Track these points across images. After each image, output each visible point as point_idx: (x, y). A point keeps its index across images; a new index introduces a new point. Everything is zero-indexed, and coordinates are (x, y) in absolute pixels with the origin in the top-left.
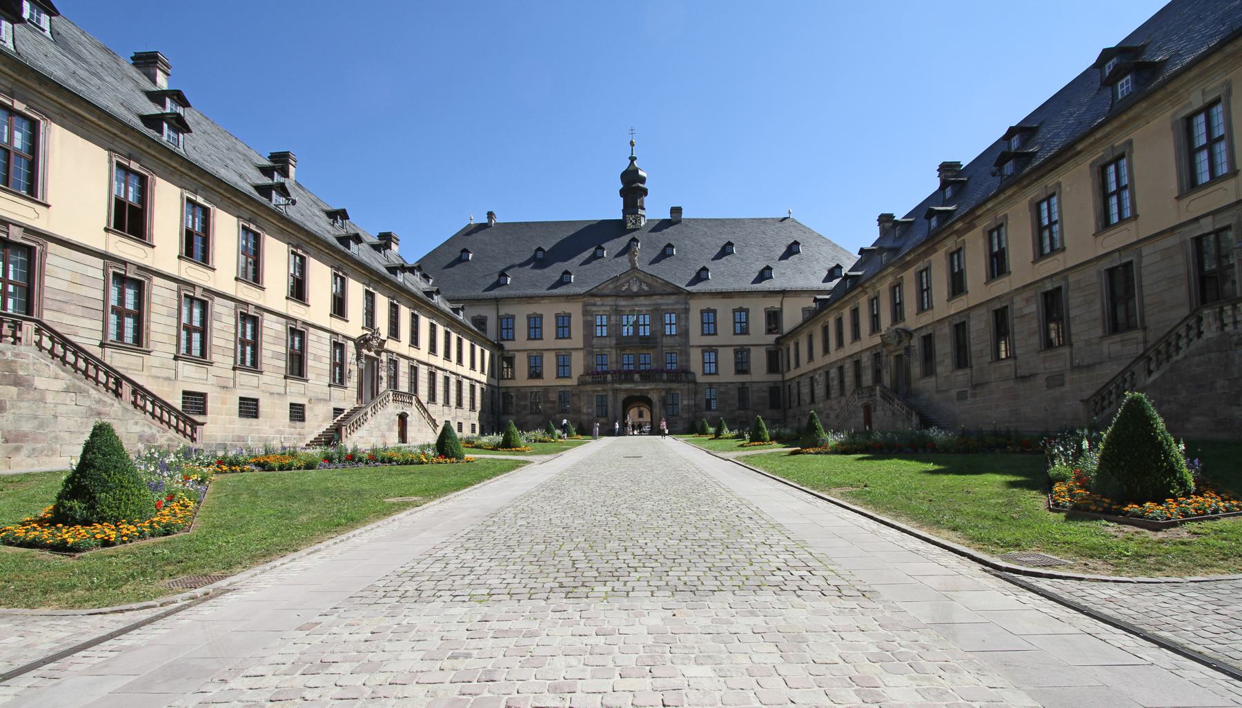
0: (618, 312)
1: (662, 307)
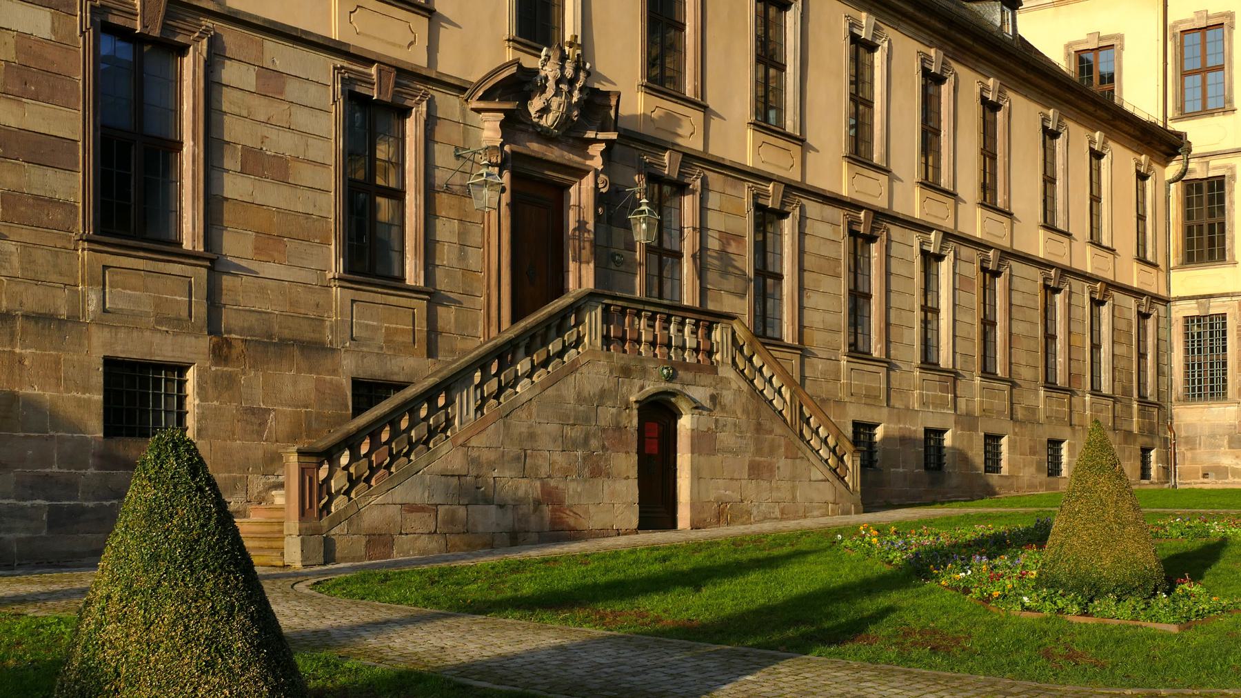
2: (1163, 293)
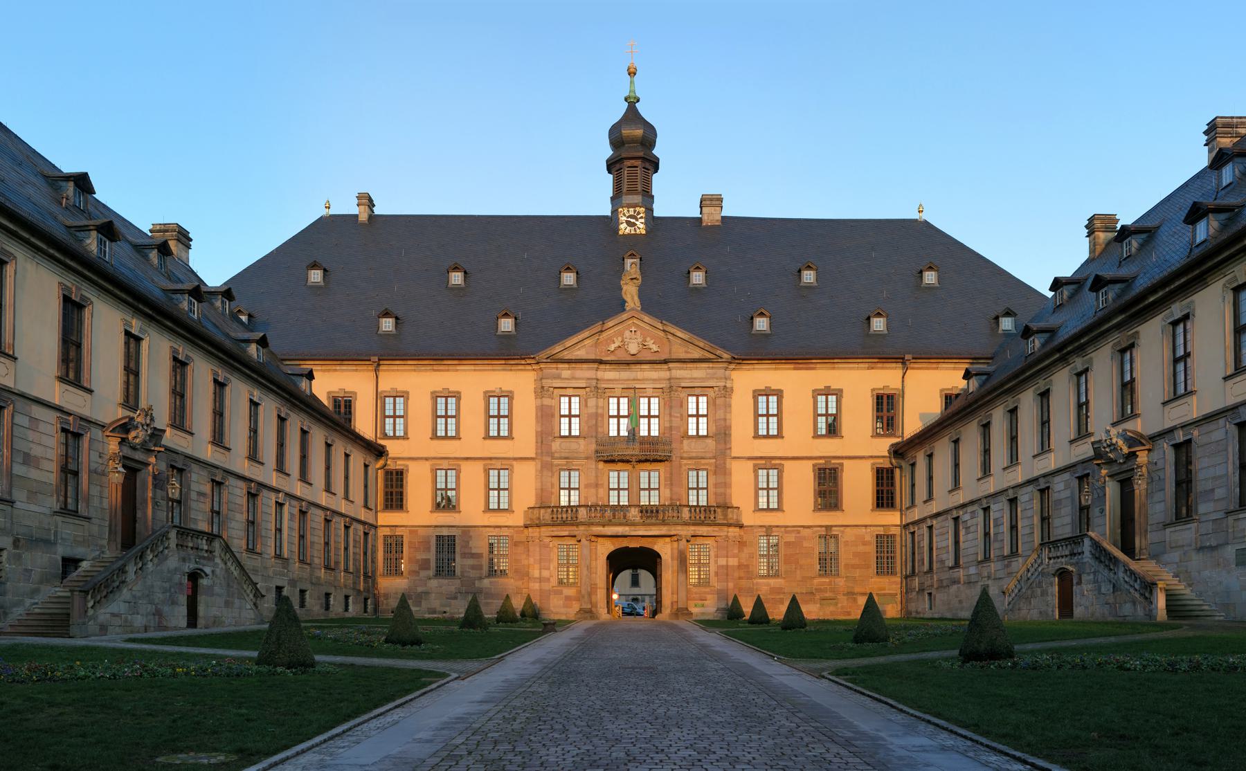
0: (599, 391)
1: (683, 385)
2: (375, 523)
